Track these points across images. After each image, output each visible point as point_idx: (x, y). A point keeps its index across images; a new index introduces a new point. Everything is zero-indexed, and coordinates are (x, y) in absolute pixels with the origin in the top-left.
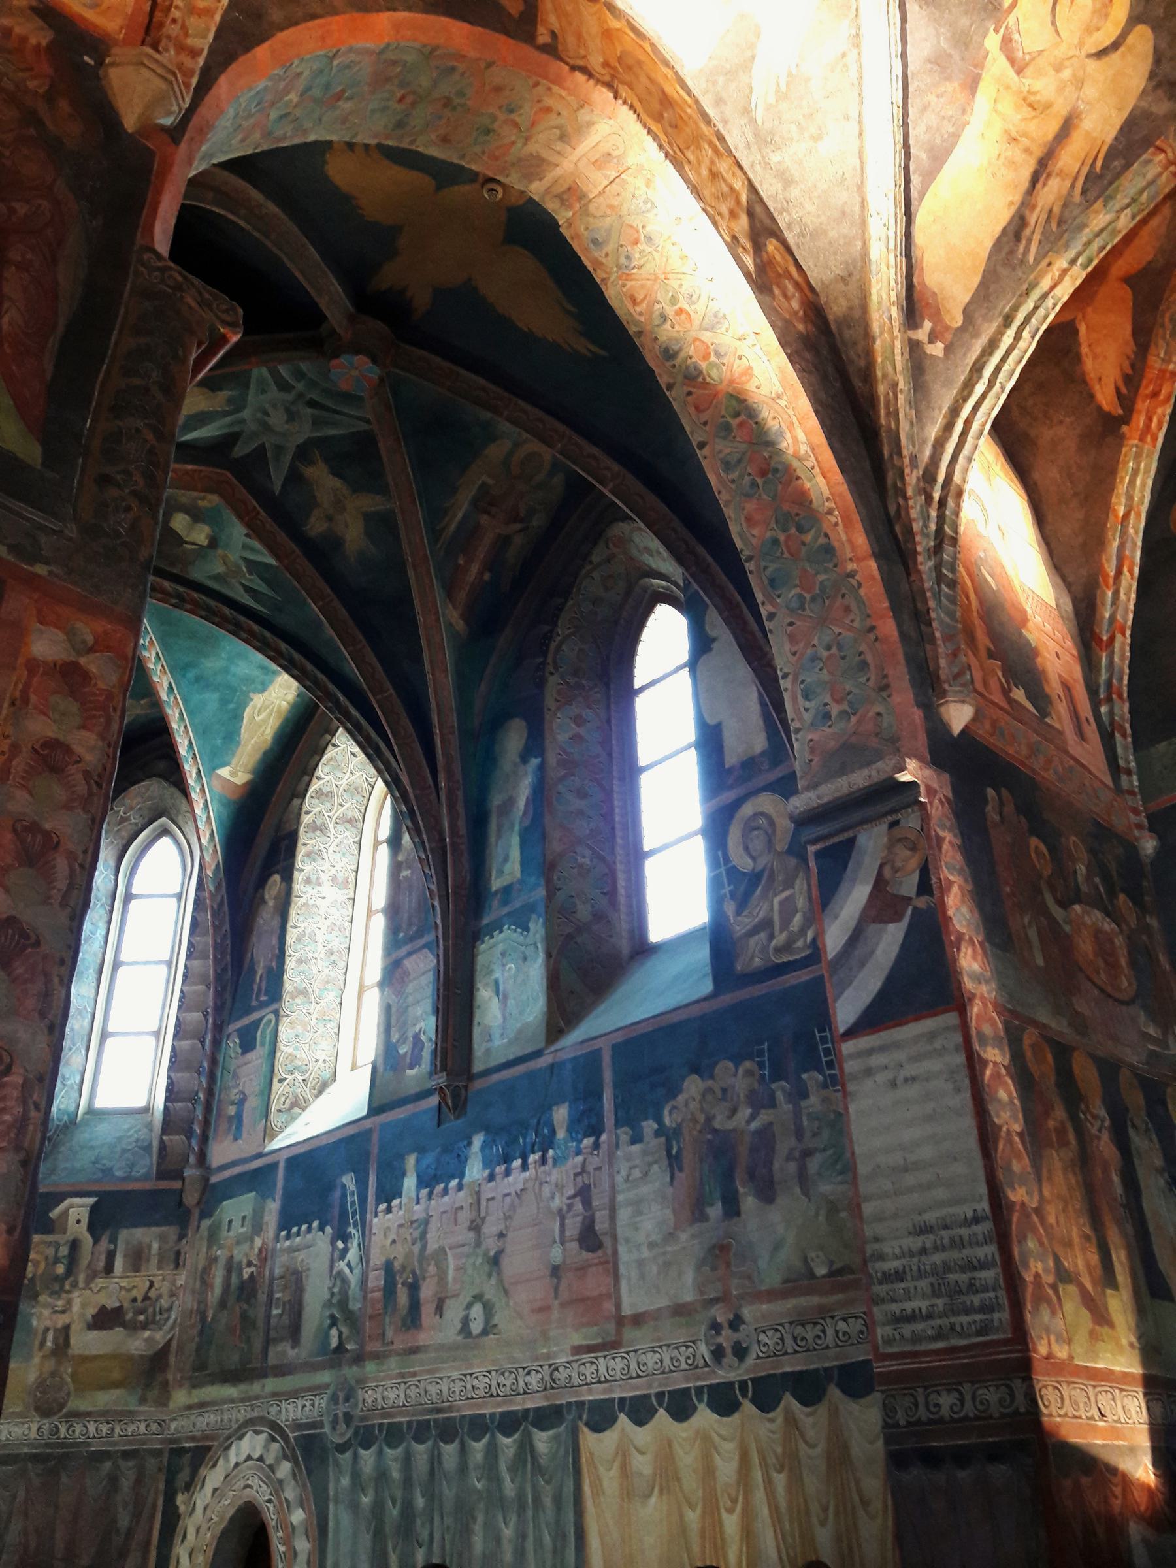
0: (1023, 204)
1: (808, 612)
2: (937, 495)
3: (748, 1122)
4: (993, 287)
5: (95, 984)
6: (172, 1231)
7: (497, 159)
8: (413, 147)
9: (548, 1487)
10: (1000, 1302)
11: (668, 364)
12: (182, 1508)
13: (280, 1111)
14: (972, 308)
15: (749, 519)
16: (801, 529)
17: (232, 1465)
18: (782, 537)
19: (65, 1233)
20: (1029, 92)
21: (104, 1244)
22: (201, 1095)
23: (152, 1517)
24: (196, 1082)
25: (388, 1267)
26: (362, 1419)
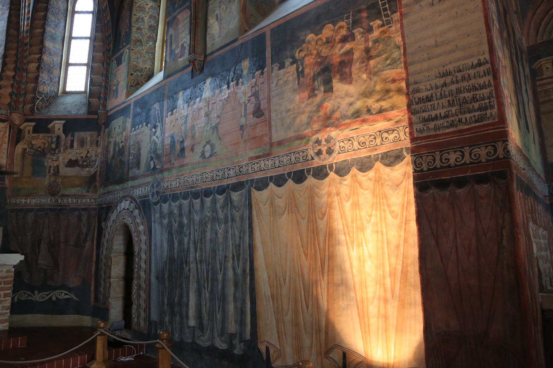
3: (340, 50)
5: (61, 44)
6: (95, 133)
9: (237, 214)
10: (492, 104)
12: (104, 227)
13: (131, 86)
17: (118, 212)
19: (54, 133)
21: (69, 138)
22: (103, 84)
23: (94, 230)
24: (101, 79)
25: (172, 137)
26: (163, 193)
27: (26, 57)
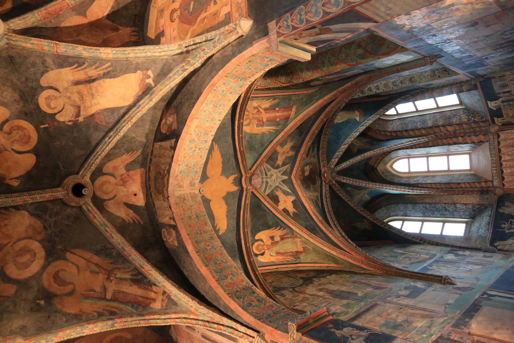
0: (101, 78)
1: (244, 77)
2: (185, 50)
4: (124, 69)
6: (493, 81)
7: (199, 208)
8: (212, 229)
11: (208, 140)
14: (133, 70)
15: (229, 100)
16: (223, 91)
18: (229, 93)
20: (80, 100)
21: (501, 95)
27: (445, 134)
